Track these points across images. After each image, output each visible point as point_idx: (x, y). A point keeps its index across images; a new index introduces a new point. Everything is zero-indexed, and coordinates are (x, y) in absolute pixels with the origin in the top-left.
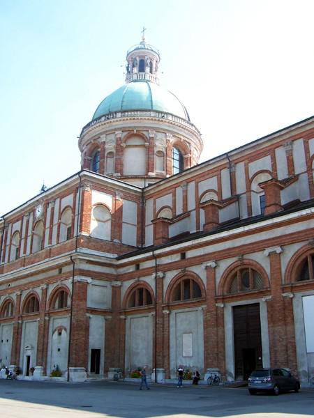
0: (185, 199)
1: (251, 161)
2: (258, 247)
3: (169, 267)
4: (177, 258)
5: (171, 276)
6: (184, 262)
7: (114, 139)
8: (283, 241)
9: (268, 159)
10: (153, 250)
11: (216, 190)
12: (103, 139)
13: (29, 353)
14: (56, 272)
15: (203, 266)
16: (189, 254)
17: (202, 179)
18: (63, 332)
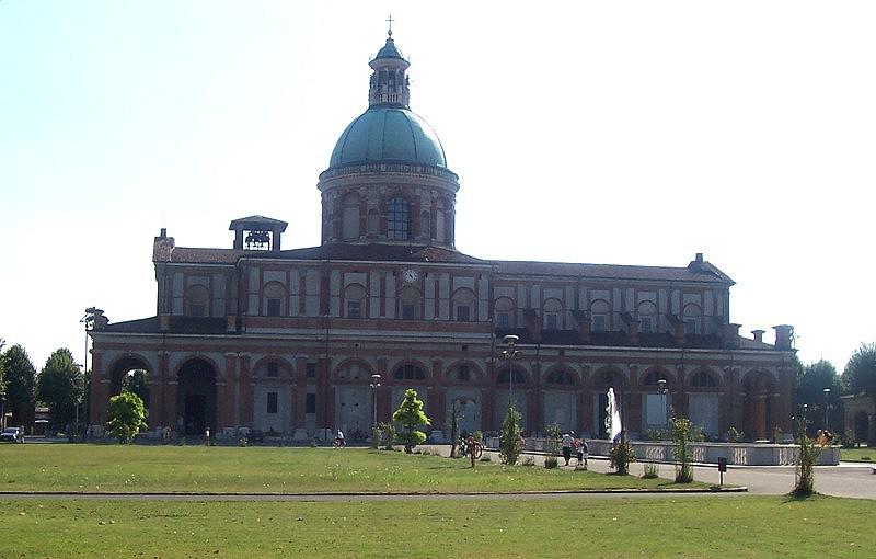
2: (623, 360)
3: (549, 359)
4: (557, 354)
5: (546, 366)
8: (639, 360)
12: (418, 192)
16: (567, 353)
18: (469, 401)
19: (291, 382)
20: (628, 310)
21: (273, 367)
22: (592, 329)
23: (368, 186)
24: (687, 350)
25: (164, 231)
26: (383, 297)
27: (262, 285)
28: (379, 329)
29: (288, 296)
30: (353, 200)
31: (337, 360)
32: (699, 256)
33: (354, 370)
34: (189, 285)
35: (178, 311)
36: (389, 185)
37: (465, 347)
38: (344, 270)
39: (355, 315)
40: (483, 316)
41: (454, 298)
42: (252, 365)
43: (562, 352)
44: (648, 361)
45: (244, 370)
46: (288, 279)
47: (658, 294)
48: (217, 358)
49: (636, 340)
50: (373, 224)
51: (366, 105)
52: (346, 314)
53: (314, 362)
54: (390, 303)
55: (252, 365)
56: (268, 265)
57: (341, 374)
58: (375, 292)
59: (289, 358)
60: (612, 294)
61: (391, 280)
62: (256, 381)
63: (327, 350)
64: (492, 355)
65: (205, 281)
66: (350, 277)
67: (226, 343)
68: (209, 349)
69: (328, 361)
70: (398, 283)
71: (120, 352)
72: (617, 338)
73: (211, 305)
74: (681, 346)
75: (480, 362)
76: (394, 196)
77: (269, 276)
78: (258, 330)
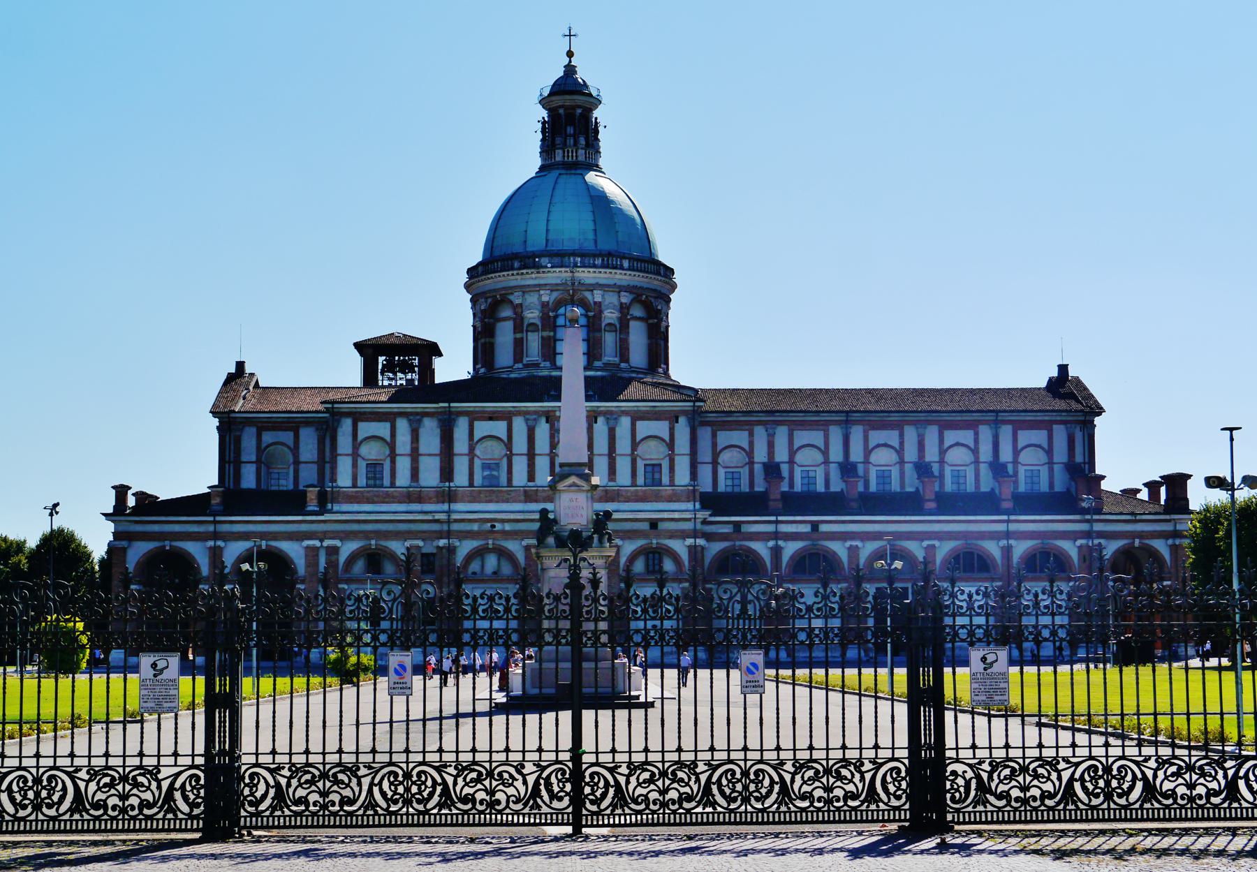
0: (771, 446)
1: (874, 428)
6: (815, 535)
7: (617, 303)
8: (940, 536)
9: (895, 433)
10: (777, 515)
11: (823, 448)
12: (598, 296)
14: (646, 526)
15: (848, 544)
16: (824, 528)
17: (799, 427)
20: (927, 459)
21: (374, 560)
22: (873, 488)
23: (525, 290)
24: (1013, 517)
25: (240, 365)
26: (531, 455)
27: (356, 445)
28: (526, 502)
29: (393, 456)
30: (507, 312)
31: (465, 548)
32: (1063, 369)
33: (491, 562)
34: (264, 445)
35: (249, 480)
36: (553, 288)
37: (654, 524)
38: (474, 417)
39: (492, 482)
40: (682, 477)
41: (640, 451)
42: (343, 558)
43: (815, 526)
44: (950, 536)
45: (332, 564)
46: (393, 434)
47: (976, 434)
48: (294, 551)
49: (932, 505)
50: (534, 342)
51: (538, 162)
52: (478, 480)
53: (435, 551)
54: (542, 464)
55: (343, 558)
56: (365, 413)
57: (475, 566)
58: (520, 445)
59: (398, 548)
60: (902, 436)
61: (543, 430)
62: (348, 581)
63: (448, 534)
64: (695, 534)
65: (287, 437)
66: (482, 428)
67: (304, 527)
69: (451, 550)
71: (151, 545)
72: (907, 503)
73: (296, 472)
74: (1008, 513)
75: (680, 547)
76: (559, 303)
77: (366, 429)
78: (345, 507)
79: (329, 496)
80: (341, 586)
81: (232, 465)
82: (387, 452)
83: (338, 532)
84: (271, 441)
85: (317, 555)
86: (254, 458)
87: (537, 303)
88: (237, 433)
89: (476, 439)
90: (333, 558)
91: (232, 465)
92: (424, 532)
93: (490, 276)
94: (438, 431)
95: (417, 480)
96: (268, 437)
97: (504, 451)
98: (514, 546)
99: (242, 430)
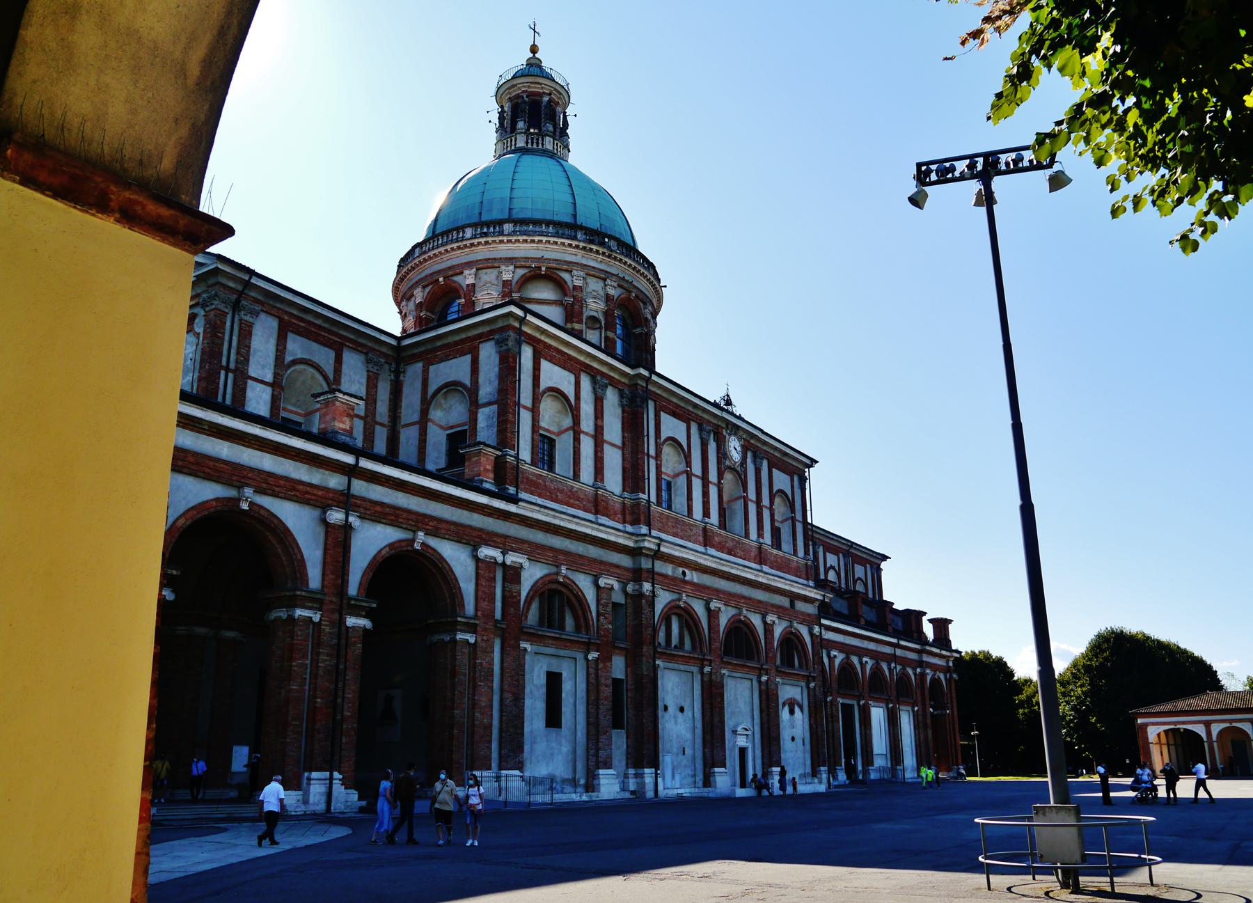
13: (742, 741)
18: (797, 709)
19: (588, 647)
34: (288, 358)
45: (510, 599)
68: (439, 528)
70: (722, 455)
79: (510, 474)
80: (524, 645)
81: (231, 376)
82: (568, 422)
83: (522, 541)
84: (299, 356)
85: (494, 579)
86: (269, 377)
87: (602, 293)
88: (248, 318)
89: (663, 439)
90: (514, 588)
91: (231, 376)
92: (617, 566)
93: (537, 238)
94: (619, 411)
95: (602, 480)
96: (296, 347)
97: (682, 467)
98: (698, 607)
99: (257, 314)
